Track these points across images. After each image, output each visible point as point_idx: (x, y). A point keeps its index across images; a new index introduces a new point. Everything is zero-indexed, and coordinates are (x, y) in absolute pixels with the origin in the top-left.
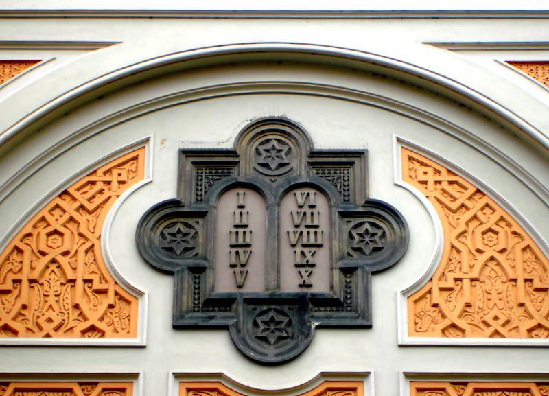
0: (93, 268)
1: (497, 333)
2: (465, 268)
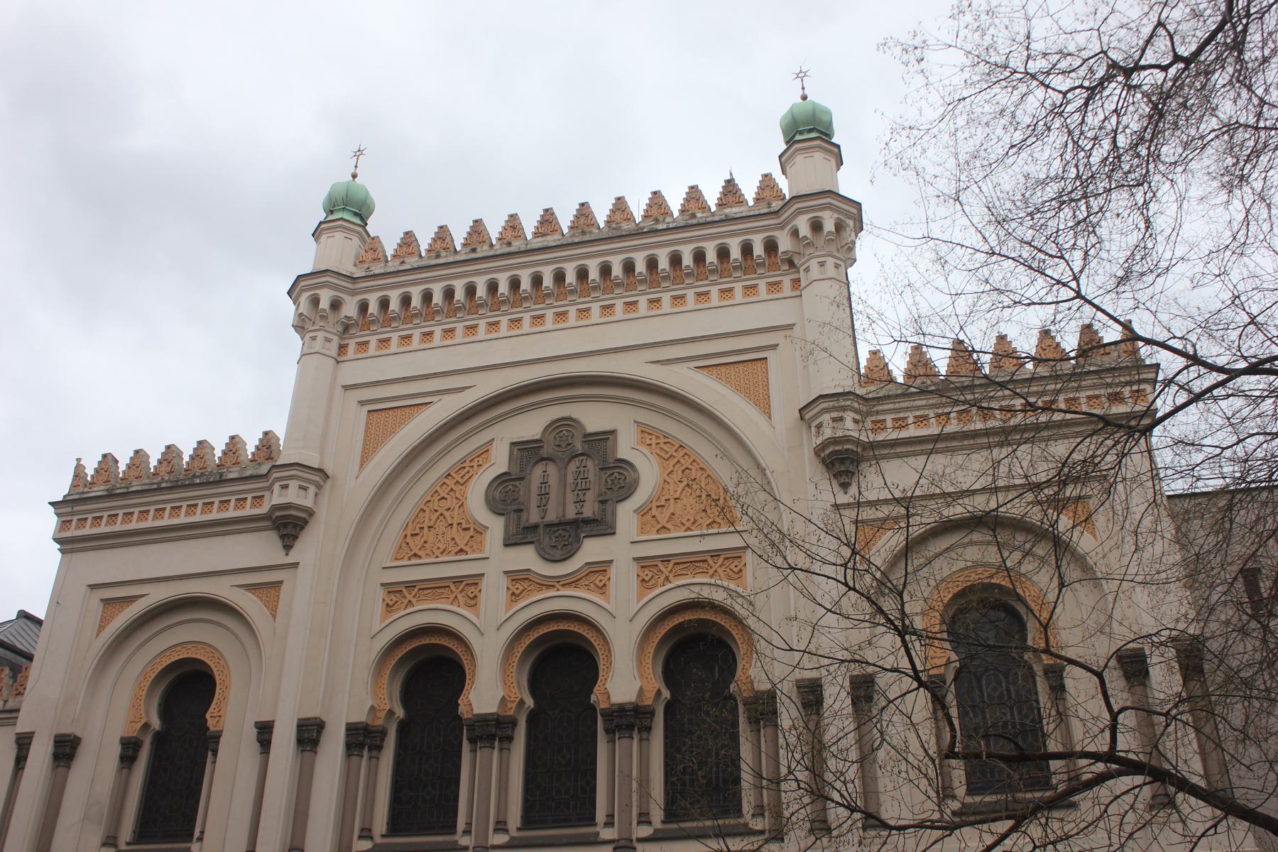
1: (688, 529)
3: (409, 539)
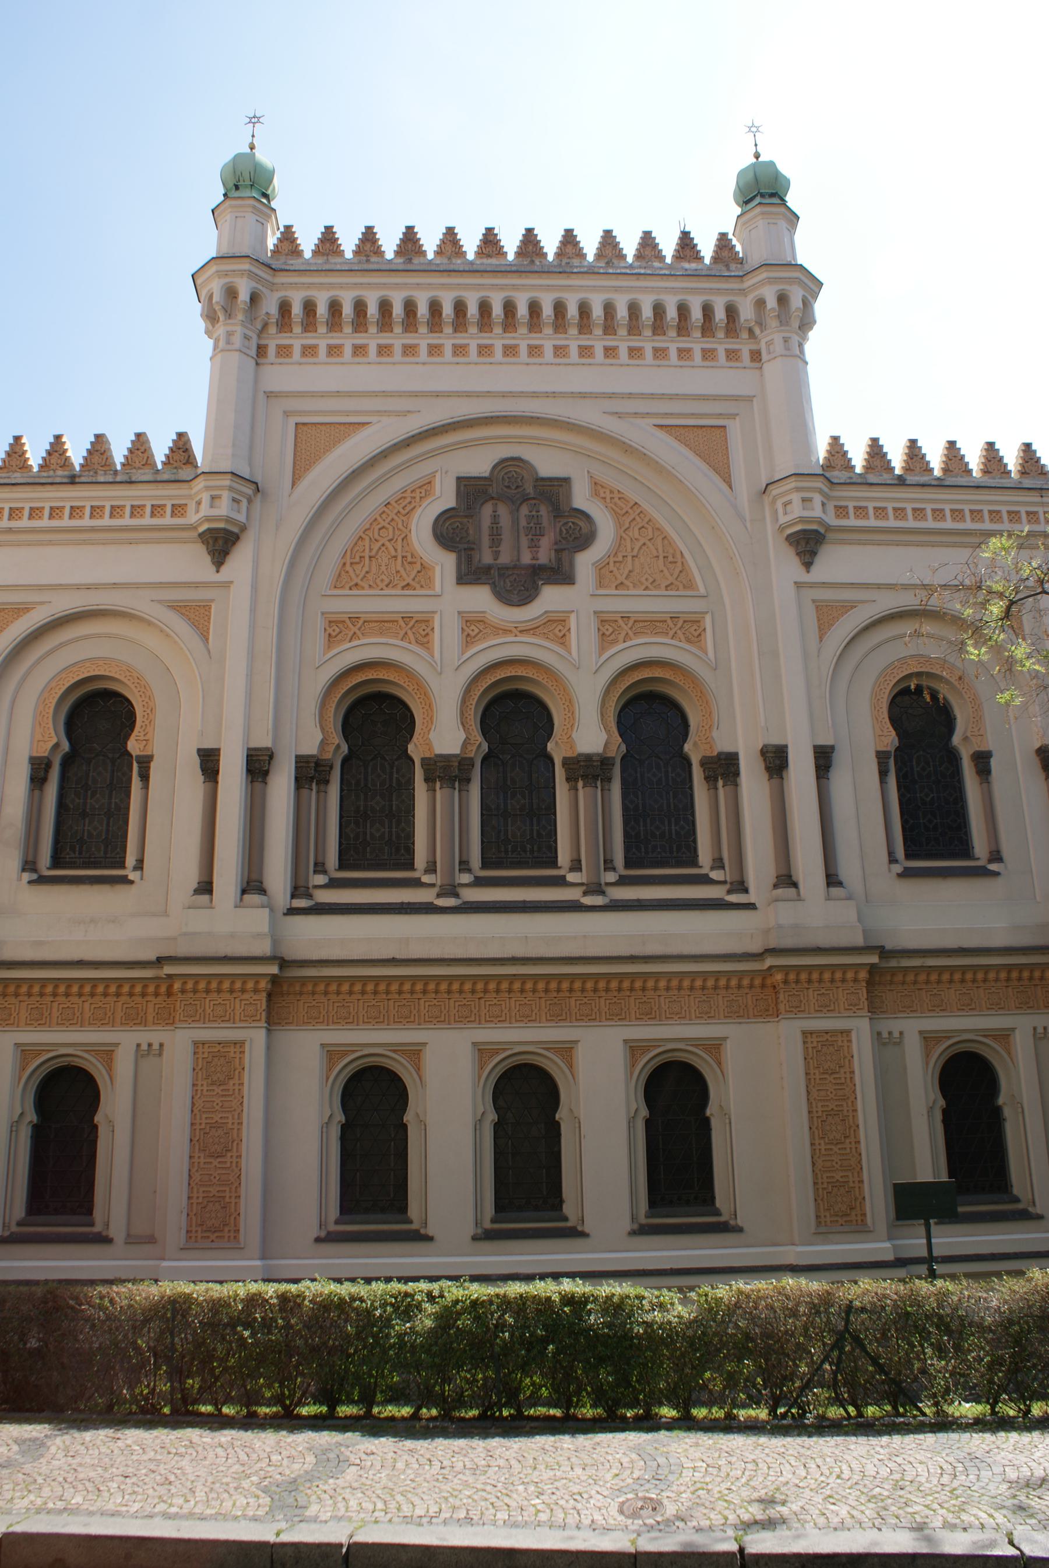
2: (629, 549)
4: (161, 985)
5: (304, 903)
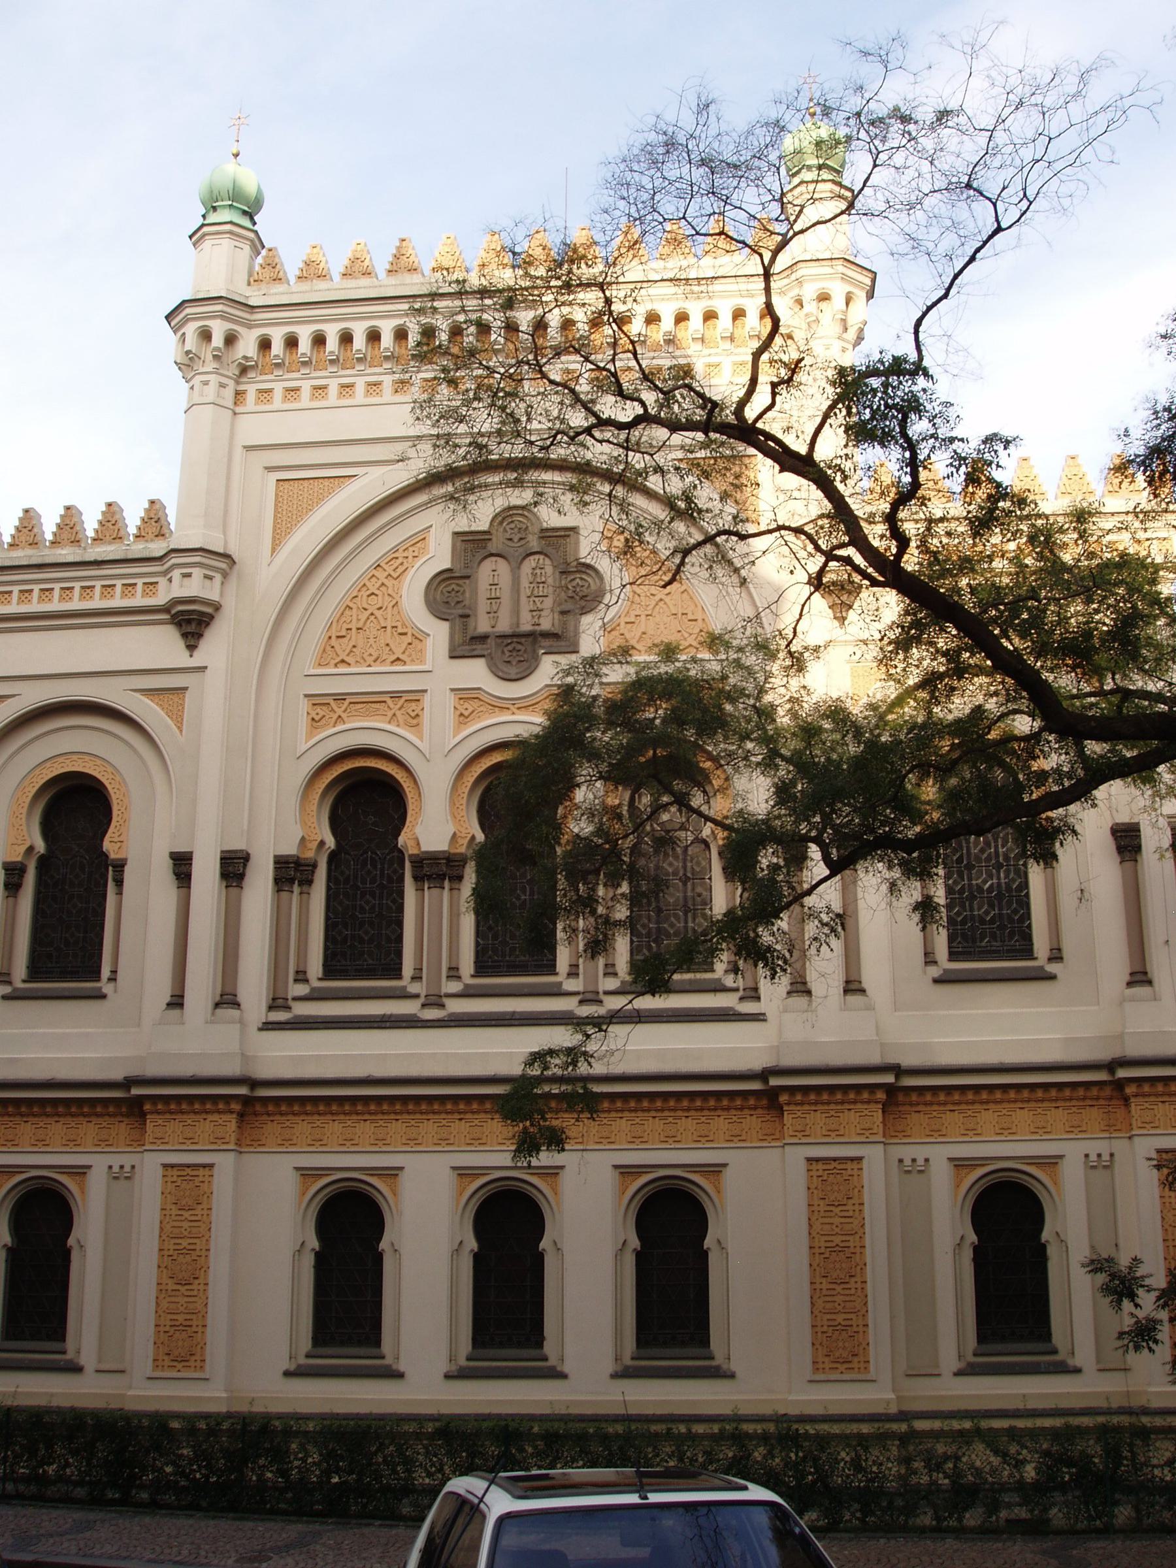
0: (398, 618)
3: (334, 642)
4: (131, 1103)
5: (283, 1018)
